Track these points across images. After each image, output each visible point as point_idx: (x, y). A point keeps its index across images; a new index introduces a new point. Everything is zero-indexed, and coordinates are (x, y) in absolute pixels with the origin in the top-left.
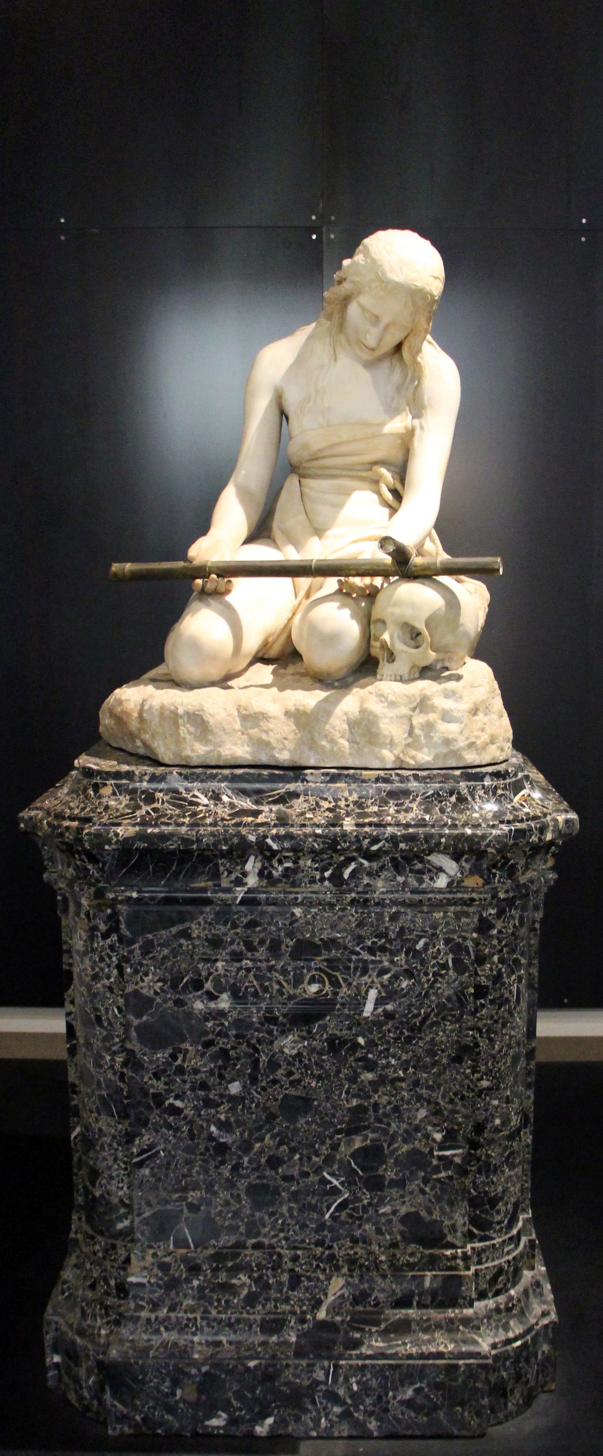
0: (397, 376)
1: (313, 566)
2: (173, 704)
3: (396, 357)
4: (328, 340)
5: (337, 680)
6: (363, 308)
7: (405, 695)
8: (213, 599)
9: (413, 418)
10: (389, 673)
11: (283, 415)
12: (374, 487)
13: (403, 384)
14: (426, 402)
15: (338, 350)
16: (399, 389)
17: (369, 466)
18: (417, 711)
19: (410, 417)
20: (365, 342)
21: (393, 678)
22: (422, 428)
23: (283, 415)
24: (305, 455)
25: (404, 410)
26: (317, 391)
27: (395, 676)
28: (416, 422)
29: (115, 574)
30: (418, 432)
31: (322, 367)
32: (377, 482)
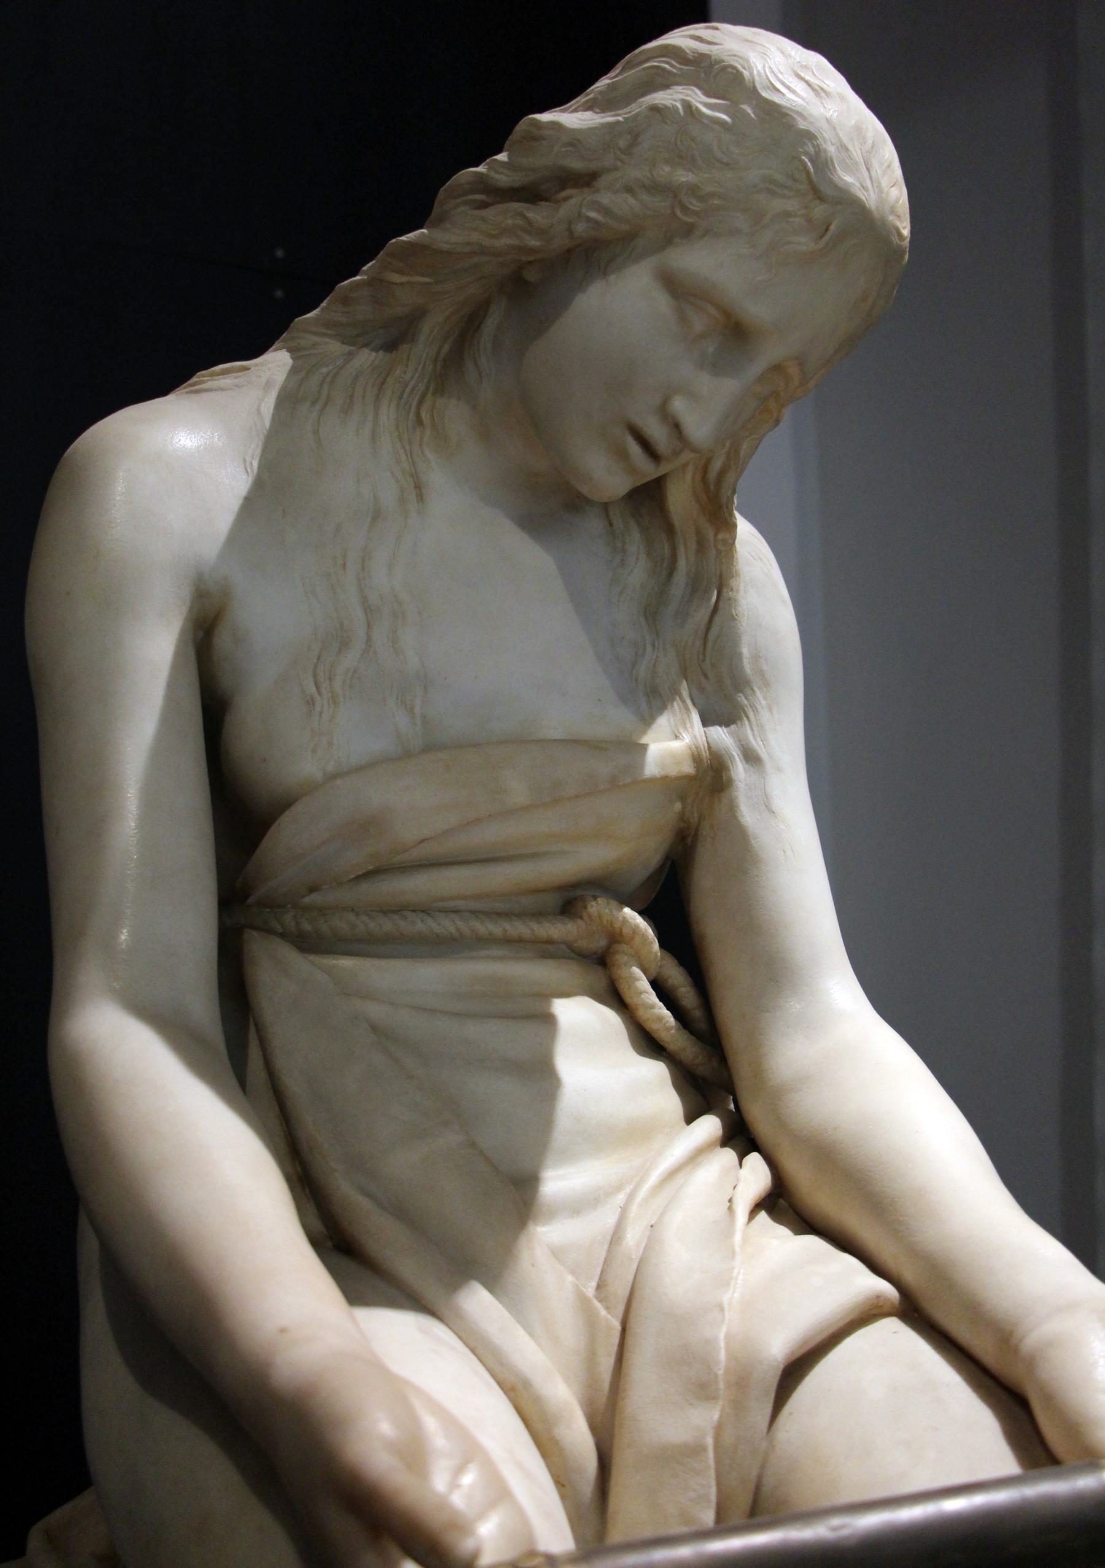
4: (388, 414)
9: (706, 722)
12: (598, 978)
14: (747, 667)
19: (696, 717)
20: (657, 432)
22: (751, 758)
25: (675, 692)
26: (368, 609)
28: (720, 735)
30: (739, 771)
31: (377, 515)
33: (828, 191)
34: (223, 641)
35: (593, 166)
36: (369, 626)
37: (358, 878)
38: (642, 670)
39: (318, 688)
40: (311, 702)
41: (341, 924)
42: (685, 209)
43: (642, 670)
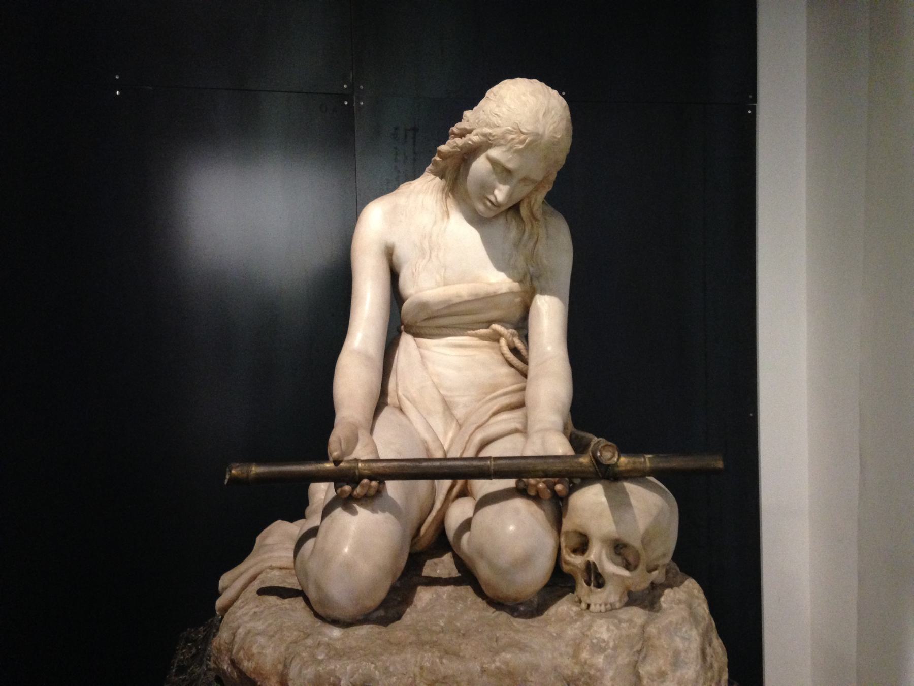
0: (513, 233)
1: (492, 468)
2: (331, 673)
3: (511, 213)
5: (521, 604)
6: (494, 162)
7: (628, 636)
8: (361, 505)
10: (600, 602)
11: (394, 276)
13: (521, 239)
15: (448, 204)
16: (517, 245)
17: (487, 324)
18: (643, 655)
21: (603, 608)
23: (394, 276)
24: (423, 315)
27: (606, 604)
29: (234, 480)
32: (498, 341)
33: (523, 130)
34: (394, 258)
35: (471, 128)
36: (431, 253)
37: (425, 319)
38: (512, 262)
39: (416, 270)
40: (413, 274)
41: (426, 331)
42: (490, 140)
43: (512, 262)
